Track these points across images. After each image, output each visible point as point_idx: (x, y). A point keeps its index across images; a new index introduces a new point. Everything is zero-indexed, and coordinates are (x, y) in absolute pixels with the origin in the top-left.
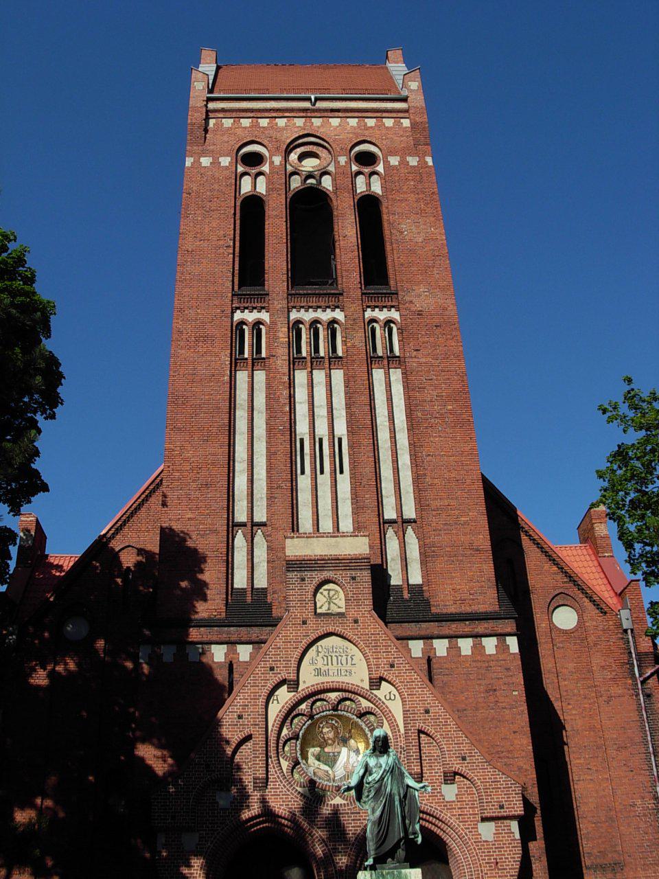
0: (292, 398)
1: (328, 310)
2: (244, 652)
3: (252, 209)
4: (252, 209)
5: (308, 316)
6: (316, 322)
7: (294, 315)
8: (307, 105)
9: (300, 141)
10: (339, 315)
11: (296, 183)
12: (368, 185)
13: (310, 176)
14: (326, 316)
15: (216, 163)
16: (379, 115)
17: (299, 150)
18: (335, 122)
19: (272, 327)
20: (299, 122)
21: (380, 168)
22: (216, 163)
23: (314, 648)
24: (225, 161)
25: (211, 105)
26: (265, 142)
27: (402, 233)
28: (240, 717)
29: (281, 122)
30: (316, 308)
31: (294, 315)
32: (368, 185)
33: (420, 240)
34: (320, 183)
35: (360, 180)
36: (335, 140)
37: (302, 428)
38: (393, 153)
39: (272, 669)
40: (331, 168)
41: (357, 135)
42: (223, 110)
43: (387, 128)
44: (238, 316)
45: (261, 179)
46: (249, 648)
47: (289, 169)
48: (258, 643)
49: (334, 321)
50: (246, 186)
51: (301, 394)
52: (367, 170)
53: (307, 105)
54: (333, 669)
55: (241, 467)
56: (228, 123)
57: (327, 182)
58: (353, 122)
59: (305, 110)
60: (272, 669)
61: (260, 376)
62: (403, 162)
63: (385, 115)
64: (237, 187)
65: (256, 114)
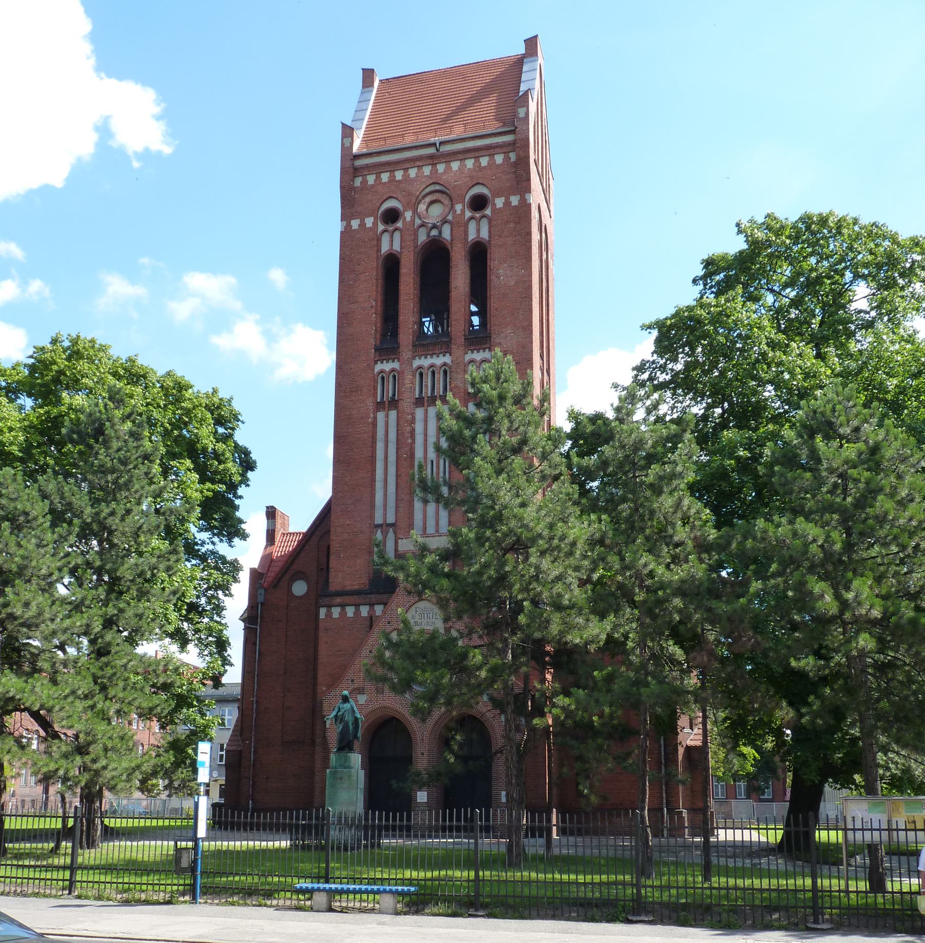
0: (414, 430)
1: (441, 355)
2: (379, 609)
3: (391, 265)
4: (391, 265)
5: (426, 362)
6: (432, 366)
7: (417, 363)
8: (431, 151)
9: (428, 190)
10: (447, 359)
11: (422, 238)
12: (478, 231)
13: (434, 226)
14: (438, 361)
15: (362, 224)
16: (492, 151)
17: (428, 200)
18: (455, 165)
19: (401, 373)
20: (427, 170)
21: (488, 212)
22: (362, 224)
23: (413, 608)
24: (369, 222)
25: (358, 163)
26: (400, 197)
27: (498, 277)
28: (371, 652)
29: (413, 173)
30: (432, 356)
31: (417, 363)
32: (478, 231)
33: (513, 283)
34: (440, 233)
35: (472, 226)
36: (455, 187)
37: (419, 454)
38: (498, 194)
39: (389, 623)
40: (450, 217)
41: (471, 177)
42: (367, 167)
43: (499, 166)
44: (379, 367)
45: (397, 235)
46: (381, 607)
47: (418, 222)
48: (385, 604)
49: (445, 364)
50: (385, 248)
51: (419, 427)
52: (478, 215)
53: (431, 151)
54: (424, 621)
55: (379, 485)
56: (371, 179)
57: (446, 233)
58: (470, 163)
59: (431, 157)
60: (389, 623)
61: (393, 414)
62: (507, 203)
63: (497, 150)
64: (379, 250)
65: (391, 166)
